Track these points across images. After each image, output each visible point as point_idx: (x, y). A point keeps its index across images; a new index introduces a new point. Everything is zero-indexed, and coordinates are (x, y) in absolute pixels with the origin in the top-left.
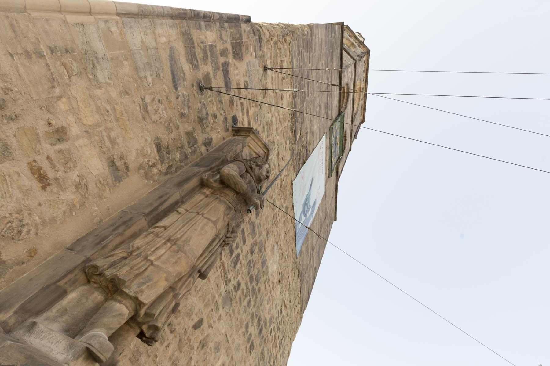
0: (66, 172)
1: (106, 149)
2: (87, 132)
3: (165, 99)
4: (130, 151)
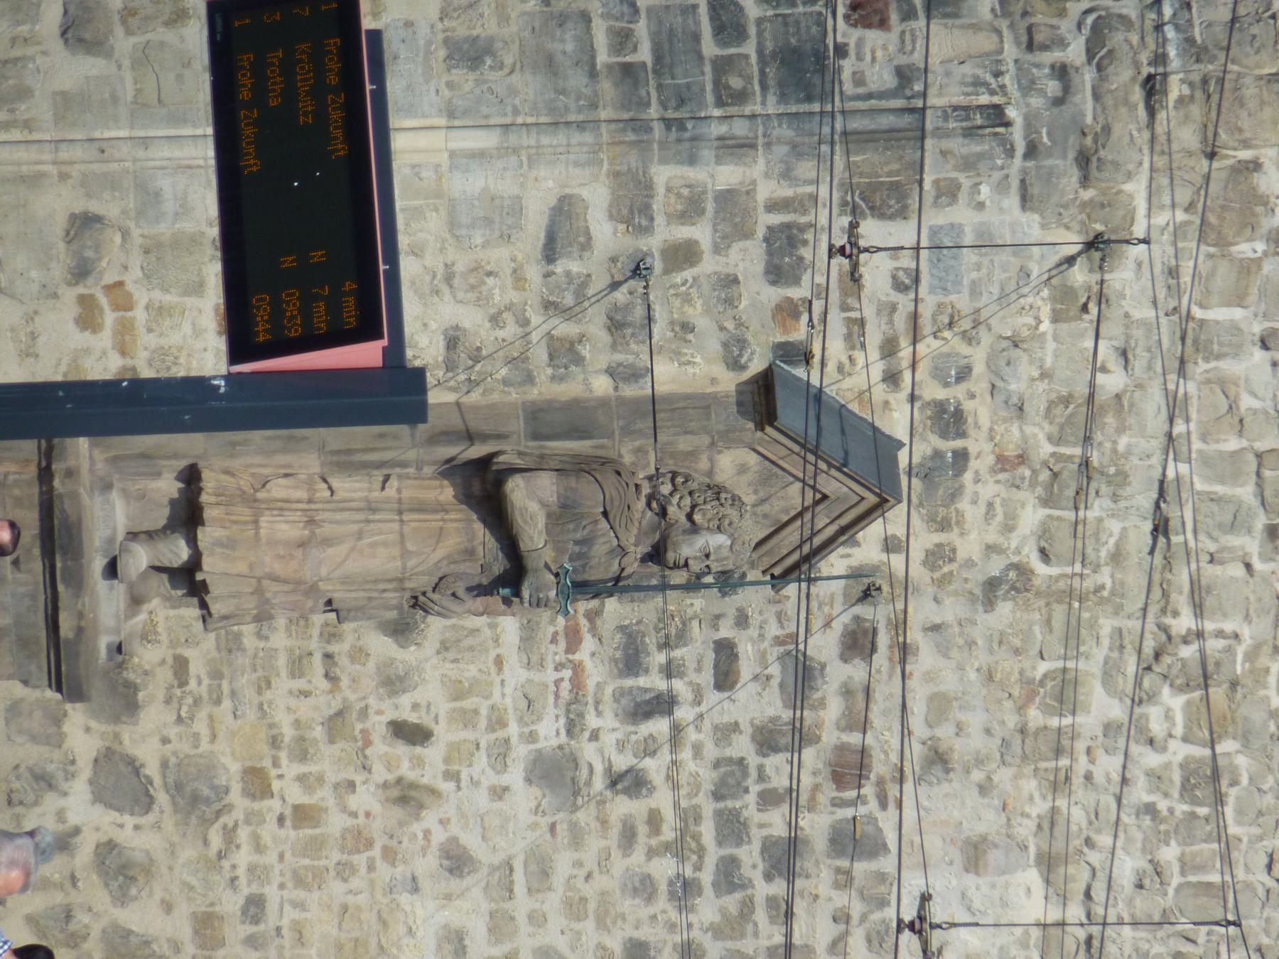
3: (509, 271)
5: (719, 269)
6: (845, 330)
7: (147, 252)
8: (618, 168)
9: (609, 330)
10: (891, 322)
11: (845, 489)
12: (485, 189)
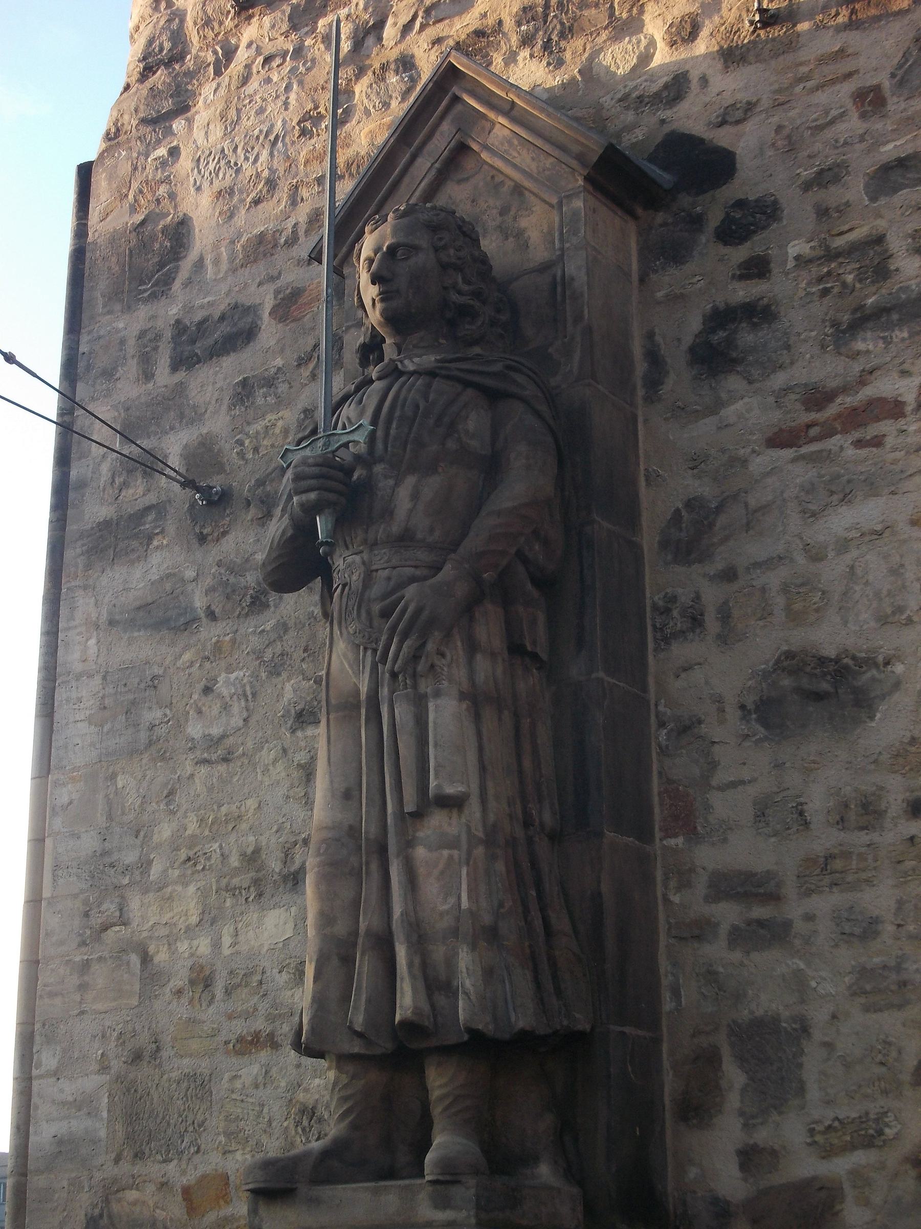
0: (265, 995)
1: (252, 889)
2: (213, 922)
3: (207, 665)
5: (224, 407)
7: (139, 1156)
8: (81, 566)
12: (90, 720)
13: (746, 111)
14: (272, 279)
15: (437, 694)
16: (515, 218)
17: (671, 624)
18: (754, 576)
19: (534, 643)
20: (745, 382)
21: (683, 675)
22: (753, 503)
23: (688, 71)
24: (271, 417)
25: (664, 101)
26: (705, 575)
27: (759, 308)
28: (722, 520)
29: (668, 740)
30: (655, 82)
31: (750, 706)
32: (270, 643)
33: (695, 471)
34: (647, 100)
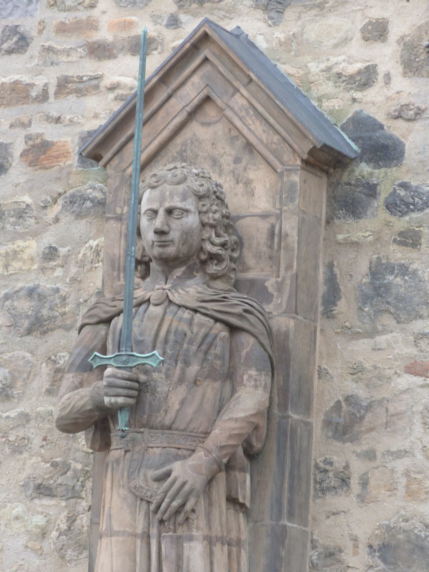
4: (22, 562)
6: (72, 98)
9: (44, 333)
10: (68, 52)
11: (195, 79)
13: (417, 114)
14: (24, 125)
15: (191, 539)
16: (245, 169)
17: (328, 481)
18: (387, 461)
19: (244, 498)
20: (395, 321)
21: (332, 517)
22: (392, 410)
23: (376, 65)
24: (20, 243)
25: (357, 84)
26: (354, 452)
27: (410, 270)
28: (368, 417)
29: (318, 559)
30: (351, 64)
31: (376, 547)
32: (13, 428)
33: (354, 376)
34: (344, 78)
